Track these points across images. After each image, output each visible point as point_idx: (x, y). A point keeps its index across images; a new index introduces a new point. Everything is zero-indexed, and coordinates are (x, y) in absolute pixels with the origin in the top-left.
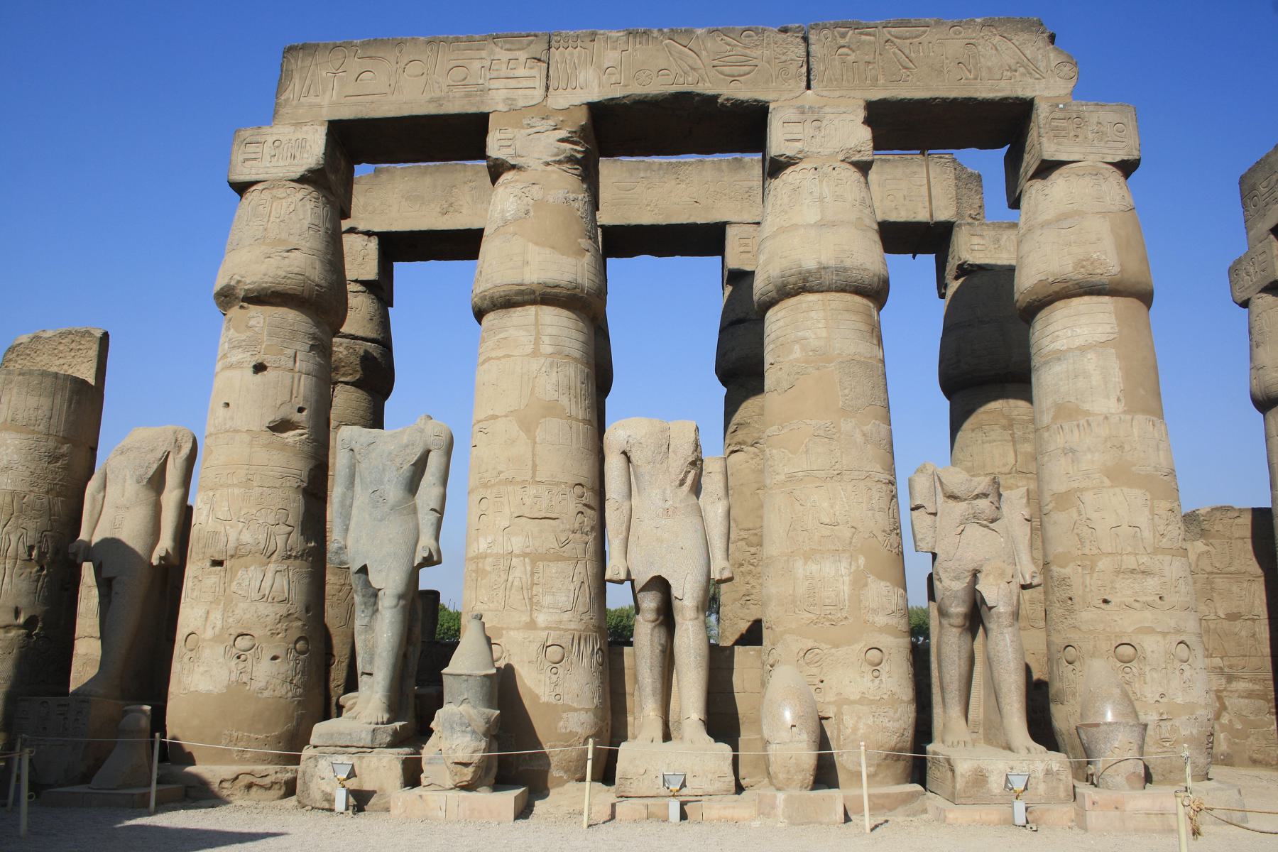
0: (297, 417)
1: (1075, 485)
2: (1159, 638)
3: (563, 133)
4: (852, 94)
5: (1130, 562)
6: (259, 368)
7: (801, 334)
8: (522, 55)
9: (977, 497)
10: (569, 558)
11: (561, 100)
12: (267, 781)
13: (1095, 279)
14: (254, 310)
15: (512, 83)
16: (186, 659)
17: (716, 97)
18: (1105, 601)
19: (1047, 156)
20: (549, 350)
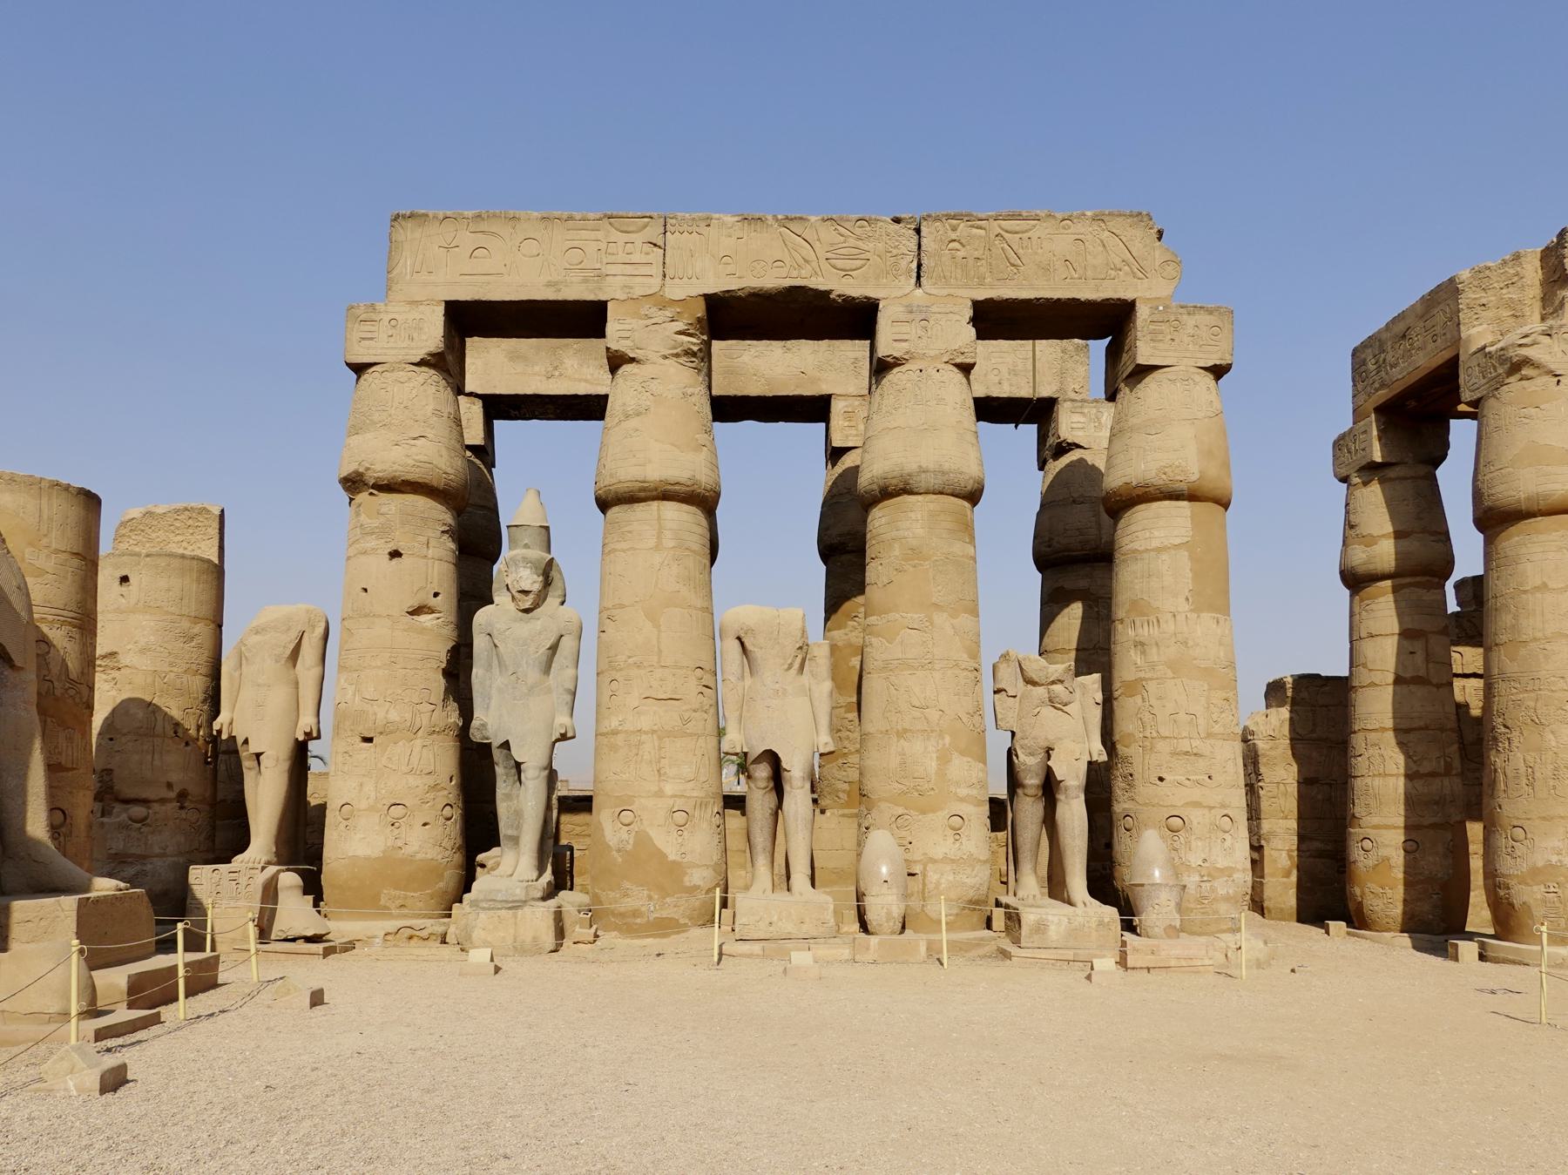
0: (433, 602)
1: (1142, 675)
2: (1206, 811)
3: (680, 326)
4: (960, 292)
5: (1185, 746)
6: (395, 554)
7: (901, 533)
8: (639, 238)
9: (1053, 683)
10: (691, 735)
11: (676, 291)
12: (424, 934)
13: (1178, 486)
14: (384, 497)
15: (629, 269)
16: (342, 827)
17: (830, 292)
18: (1161, 779)
19: (1141, 360)
20: (671, 544)
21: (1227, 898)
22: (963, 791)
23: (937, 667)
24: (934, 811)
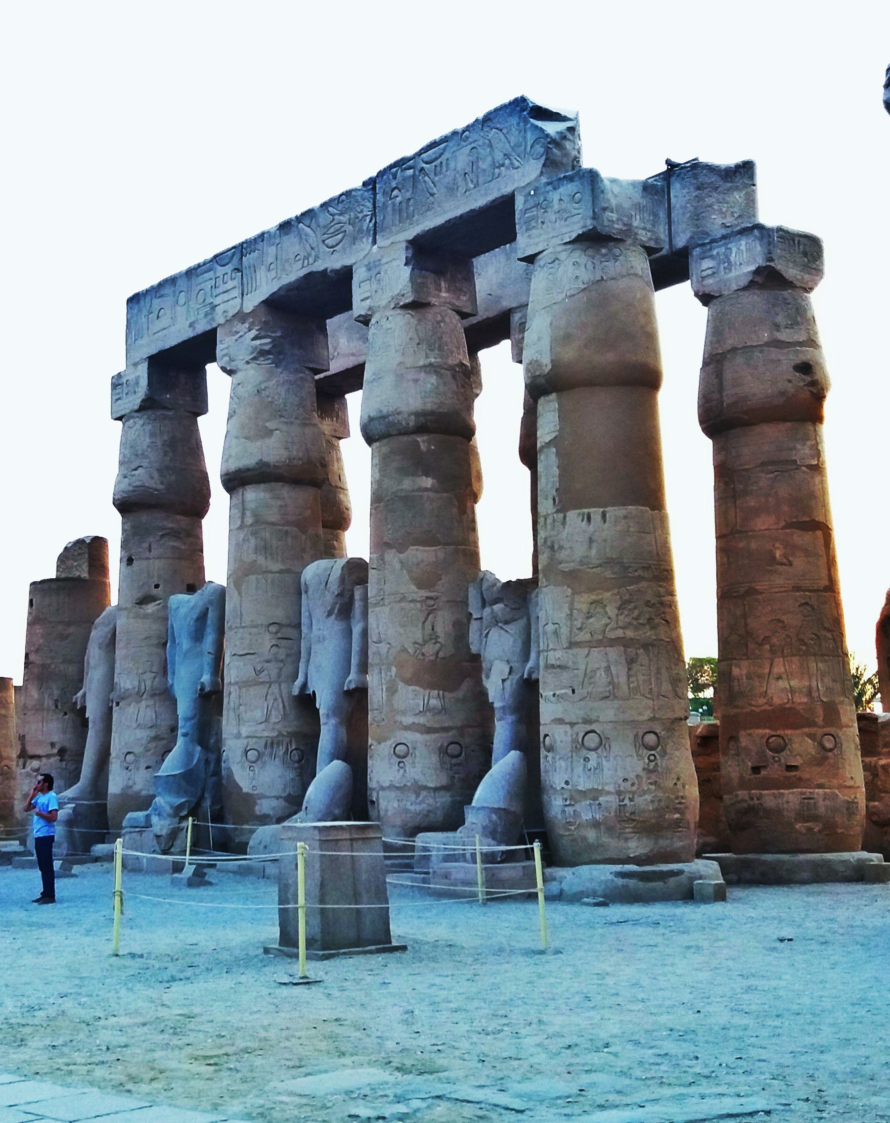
3: (254, 333)
21: (596, 824)
22: (408, 720)
23: (386, 602)
24: (385, 741)
